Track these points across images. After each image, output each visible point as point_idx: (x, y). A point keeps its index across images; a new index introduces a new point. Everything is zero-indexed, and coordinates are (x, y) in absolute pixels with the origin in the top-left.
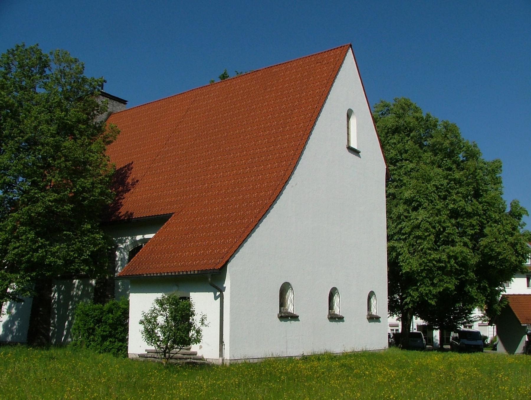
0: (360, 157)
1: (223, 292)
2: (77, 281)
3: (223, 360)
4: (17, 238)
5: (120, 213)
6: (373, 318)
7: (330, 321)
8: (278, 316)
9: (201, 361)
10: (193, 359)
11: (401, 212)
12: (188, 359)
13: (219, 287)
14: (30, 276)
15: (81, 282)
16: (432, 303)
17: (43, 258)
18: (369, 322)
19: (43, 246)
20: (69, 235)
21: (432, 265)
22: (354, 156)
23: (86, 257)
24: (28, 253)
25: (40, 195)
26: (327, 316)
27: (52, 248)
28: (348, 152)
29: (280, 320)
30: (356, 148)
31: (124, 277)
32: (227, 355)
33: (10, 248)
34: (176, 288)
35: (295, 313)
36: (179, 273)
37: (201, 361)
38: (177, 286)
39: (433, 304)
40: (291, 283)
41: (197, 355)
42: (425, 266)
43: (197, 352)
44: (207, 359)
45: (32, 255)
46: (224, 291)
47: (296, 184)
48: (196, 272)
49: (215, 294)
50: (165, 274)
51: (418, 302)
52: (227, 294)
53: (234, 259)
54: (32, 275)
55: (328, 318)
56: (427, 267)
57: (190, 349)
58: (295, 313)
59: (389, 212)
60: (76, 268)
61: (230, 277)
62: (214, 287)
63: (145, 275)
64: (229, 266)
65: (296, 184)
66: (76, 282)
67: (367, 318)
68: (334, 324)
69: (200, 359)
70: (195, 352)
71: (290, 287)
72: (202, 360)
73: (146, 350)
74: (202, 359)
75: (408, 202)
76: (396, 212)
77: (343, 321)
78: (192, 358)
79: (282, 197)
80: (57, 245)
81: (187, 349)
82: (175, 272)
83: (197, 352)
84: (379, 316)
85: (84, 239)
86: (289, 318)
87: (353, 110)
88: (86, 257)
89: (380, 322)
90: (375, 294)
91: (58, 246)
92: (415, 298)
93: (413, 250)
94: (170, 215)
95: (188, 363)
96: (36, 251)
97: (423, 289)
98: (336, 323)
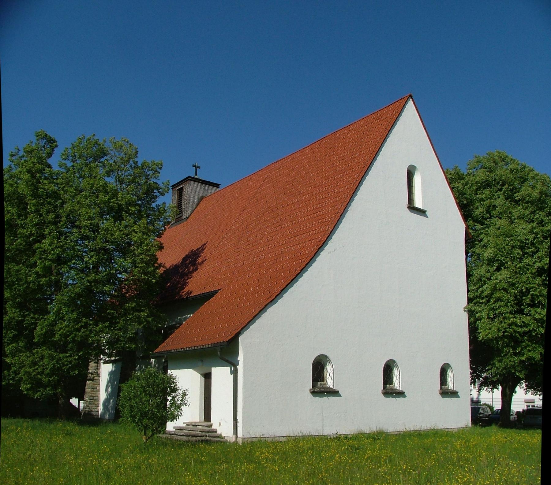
0: (428, 218)
1: (238, 366)
2: (154, 360)
3: (237, 438)
4: (62, 319)
5: (183, 292)
6: (446, 393)
8: (310, 391)
9: (219, 439)
10: (209, 437)
11: (482, 274)
12: (203, 436)
13: (233, 361)
14: (78, 355)
15: (156, 361)
16: (521, 376)
18: (443, 398)
19: (86, 326)
20: (113, 313)
21: (512, 331)
22: (419, 216)
24: (71, 333)
26: (381, 391)
27: (95, 328)
28: (410, 212)
30: (421, 208)
32: (240, 434)
33: (56, 328)
35: (334, 388)
37: (219, 439)
38: (202, 361)
40: (328, 355)
42: (504, 332)
43: (217, 429)
44: (225, 437)
47: (335, 250)
48: (210, 346)
49: (231, 369)
50: (188, 349)
51: (504, 374)
52: (240, 368)
54: (80, 354)
56: (507, 334)
57: (212, 426)
58: (334, 388)
59: (469, 275)
62: (224, 360)
63: (173, 351)
64: (241, 338)
65: (335, 250)
66: (153, 360)
67: (440, 393)
68: (319, 400)
69: (218, 437)
70: (214, 429)
71: (328, 360)
72: (220, 438)
73: (174, 428)
74: (220, 436)
75: (490, 262)
77: (405, 396)
79: (314, 265)
80: (100, 324)
81: (207, 426)
82: (203, 345)
83: (217, 429)
84: (458, 391)
85: (128, 317)
86: (325, 393)
87: (416, 166)
88: (131, 335)
89: (459, 397)
91: (101, 325)
92: (500, 370)
93: (494, 315)
94: (217, 291)
95: (202, 441)
96: (78, 330)
97: (508, 361)
98: (394, 398)
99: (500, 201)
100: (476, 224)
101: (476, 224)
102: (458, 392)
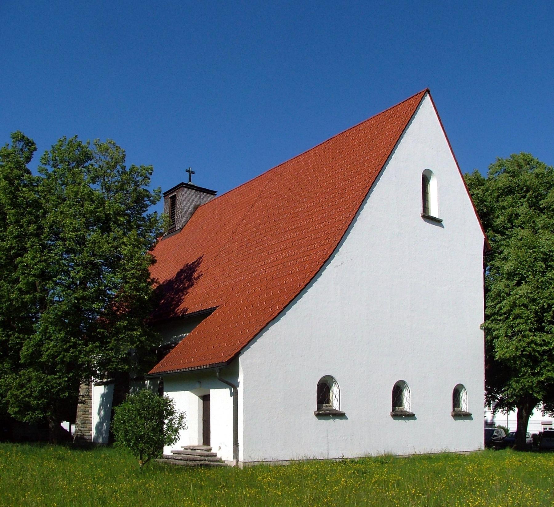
0: (444, 228)
1: (238, 388)
2: (148, 381)
3: (237, 462)
4: (49, 338)
5: (178, 310)
6: (459, 415)
7: (319, 419)
8: (315, 413)
9: (219, 463)
10: (208, 461)
11: (501, 289)
12: (203, 460)
13: (233, 383)
14: (67, 377)
15: (151, 383)
16: (538, 397)
17: (77, 357)
19: (75, 346)
20: (103, 332)
21: (531, 350)
22: (434, 225)
23: (123, 355)
24: (60, 353)
25: (64, 293)
26: (390, 413)
27: (84, 348)
28: (424, 222)
29: (317, 418)
30: (437, 217)
31: (155, 374)
32: (241, 458)
33: (43, 348)
34: (198, 385)
35: (340, 411)
36: (195, 369)
37: (219, 463)
38: (200, 382)
39: (540, 399)
40: (334, 376)
41: (217, 457)
42: (522, 351)
43: (216, 454)
44: (225, 461)
45: (64, 355)
46: (238, 387)
47: (342, 264)
48: (208, 366)
49: (231, 391)
50: (184, 370)
51: (521, 395)
52: (240, 389)
53: (248, 350)
54: (69, 376)
55: (391, 415)
56: (526, 353)
57: (211, 450)
58: (340, 411)
59: (487, 290)
60: (114, 367)
61: (243, 370)
62: (223, 382)
63: (169, 372)
64: (241, 358)
65: (342, 264)
67: (452, 416)
69: (218, 461)
70: (214, 453)
71: (334, 381)
72: (220, 462)
73: (171, 452)
74: (220, 460)
75: (510, 275)
76: (494, 289)
78: (207, 460)
79: (320, 280)
80: (90, 344)
81: (206, 450)
82: (201, 366)
83: (216, 454)
84: (471, 413)
85: (120, 337)
86: (331, 416)
87: (432, 170)
88: (123, 355)
89: (473, 420)
90: (464, 388)
91: (91, 345)
92: (517, 391)
93: (512, 333)
94: (215, 308)
95: (201, 465)
96: (67, 350)
97: (525, 381)
98: (404, 421)
99: (523, 209)
100: (496, 235)
101: (496, 235)
102: (471, 415)
